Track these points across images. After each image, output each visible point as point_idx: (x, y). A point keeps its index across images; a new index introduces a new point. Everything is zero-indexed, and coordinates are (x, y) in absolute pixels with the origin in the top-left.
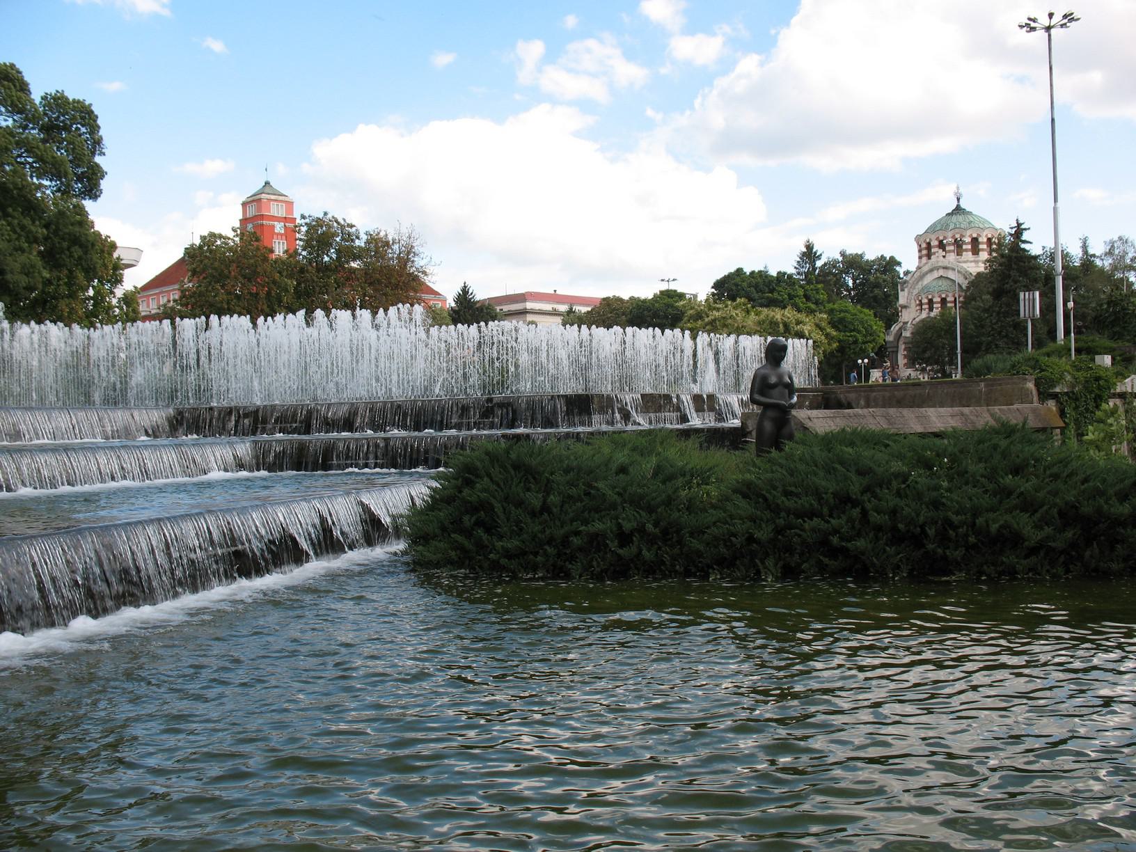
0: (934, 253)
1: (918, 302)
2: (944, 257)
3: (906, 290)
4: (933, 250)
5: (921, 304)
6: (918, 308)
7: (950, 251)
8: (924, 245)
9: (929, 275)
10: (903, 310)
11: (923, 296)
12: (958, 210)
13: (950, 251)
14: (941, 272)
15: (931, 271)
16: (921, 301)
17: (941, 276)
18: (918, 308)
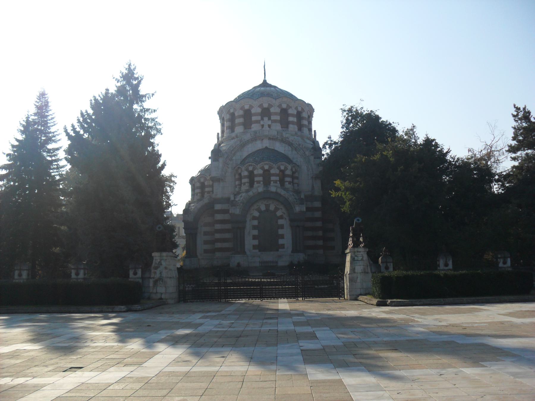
0: (257, 122)
1: (237, 177)
2: (269, 126)
3: (221, 160)
4: (254, 118)
5: (240, 179)
6: (237, 183)
7: (275, 121)
8: (227, 117)
9: (250, 145)
10: (216, 185)
11: (243, 168)
12: (265, 84)
13: (275, 121)
14: (266, 143)
15: (254, 139)
16: (240, 174)
17: (266, 148)
18: (237, 183)
